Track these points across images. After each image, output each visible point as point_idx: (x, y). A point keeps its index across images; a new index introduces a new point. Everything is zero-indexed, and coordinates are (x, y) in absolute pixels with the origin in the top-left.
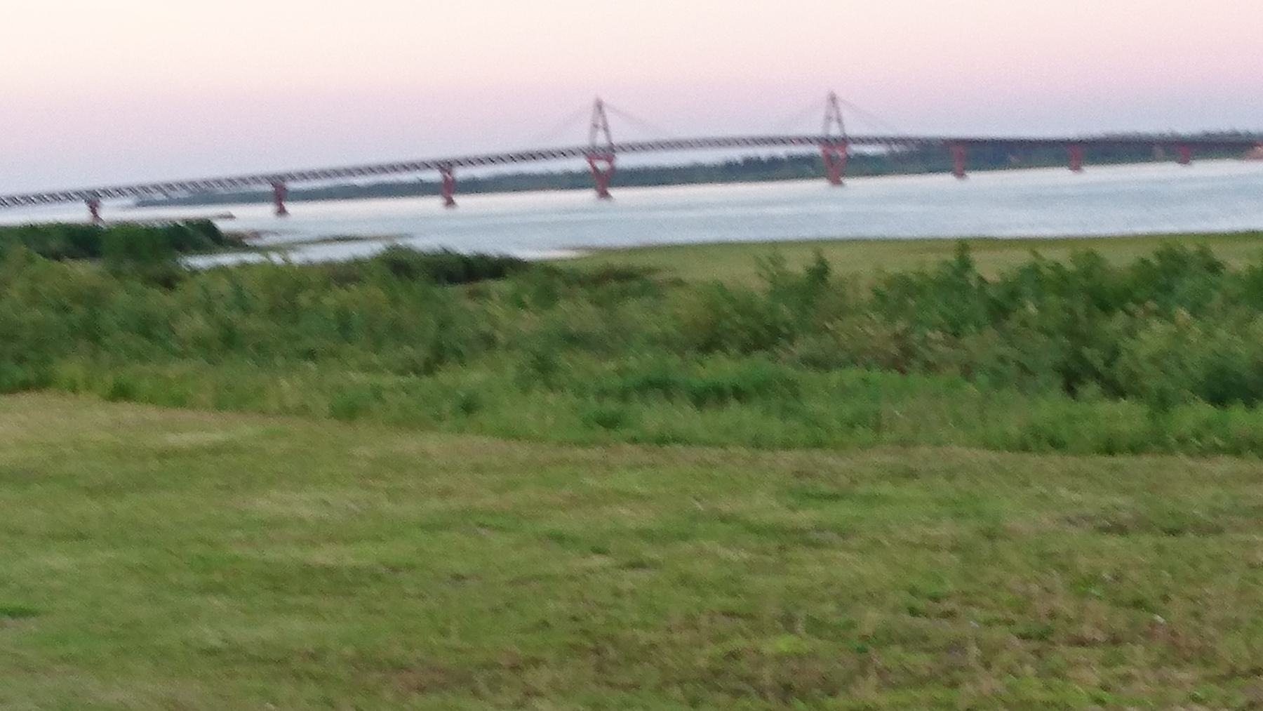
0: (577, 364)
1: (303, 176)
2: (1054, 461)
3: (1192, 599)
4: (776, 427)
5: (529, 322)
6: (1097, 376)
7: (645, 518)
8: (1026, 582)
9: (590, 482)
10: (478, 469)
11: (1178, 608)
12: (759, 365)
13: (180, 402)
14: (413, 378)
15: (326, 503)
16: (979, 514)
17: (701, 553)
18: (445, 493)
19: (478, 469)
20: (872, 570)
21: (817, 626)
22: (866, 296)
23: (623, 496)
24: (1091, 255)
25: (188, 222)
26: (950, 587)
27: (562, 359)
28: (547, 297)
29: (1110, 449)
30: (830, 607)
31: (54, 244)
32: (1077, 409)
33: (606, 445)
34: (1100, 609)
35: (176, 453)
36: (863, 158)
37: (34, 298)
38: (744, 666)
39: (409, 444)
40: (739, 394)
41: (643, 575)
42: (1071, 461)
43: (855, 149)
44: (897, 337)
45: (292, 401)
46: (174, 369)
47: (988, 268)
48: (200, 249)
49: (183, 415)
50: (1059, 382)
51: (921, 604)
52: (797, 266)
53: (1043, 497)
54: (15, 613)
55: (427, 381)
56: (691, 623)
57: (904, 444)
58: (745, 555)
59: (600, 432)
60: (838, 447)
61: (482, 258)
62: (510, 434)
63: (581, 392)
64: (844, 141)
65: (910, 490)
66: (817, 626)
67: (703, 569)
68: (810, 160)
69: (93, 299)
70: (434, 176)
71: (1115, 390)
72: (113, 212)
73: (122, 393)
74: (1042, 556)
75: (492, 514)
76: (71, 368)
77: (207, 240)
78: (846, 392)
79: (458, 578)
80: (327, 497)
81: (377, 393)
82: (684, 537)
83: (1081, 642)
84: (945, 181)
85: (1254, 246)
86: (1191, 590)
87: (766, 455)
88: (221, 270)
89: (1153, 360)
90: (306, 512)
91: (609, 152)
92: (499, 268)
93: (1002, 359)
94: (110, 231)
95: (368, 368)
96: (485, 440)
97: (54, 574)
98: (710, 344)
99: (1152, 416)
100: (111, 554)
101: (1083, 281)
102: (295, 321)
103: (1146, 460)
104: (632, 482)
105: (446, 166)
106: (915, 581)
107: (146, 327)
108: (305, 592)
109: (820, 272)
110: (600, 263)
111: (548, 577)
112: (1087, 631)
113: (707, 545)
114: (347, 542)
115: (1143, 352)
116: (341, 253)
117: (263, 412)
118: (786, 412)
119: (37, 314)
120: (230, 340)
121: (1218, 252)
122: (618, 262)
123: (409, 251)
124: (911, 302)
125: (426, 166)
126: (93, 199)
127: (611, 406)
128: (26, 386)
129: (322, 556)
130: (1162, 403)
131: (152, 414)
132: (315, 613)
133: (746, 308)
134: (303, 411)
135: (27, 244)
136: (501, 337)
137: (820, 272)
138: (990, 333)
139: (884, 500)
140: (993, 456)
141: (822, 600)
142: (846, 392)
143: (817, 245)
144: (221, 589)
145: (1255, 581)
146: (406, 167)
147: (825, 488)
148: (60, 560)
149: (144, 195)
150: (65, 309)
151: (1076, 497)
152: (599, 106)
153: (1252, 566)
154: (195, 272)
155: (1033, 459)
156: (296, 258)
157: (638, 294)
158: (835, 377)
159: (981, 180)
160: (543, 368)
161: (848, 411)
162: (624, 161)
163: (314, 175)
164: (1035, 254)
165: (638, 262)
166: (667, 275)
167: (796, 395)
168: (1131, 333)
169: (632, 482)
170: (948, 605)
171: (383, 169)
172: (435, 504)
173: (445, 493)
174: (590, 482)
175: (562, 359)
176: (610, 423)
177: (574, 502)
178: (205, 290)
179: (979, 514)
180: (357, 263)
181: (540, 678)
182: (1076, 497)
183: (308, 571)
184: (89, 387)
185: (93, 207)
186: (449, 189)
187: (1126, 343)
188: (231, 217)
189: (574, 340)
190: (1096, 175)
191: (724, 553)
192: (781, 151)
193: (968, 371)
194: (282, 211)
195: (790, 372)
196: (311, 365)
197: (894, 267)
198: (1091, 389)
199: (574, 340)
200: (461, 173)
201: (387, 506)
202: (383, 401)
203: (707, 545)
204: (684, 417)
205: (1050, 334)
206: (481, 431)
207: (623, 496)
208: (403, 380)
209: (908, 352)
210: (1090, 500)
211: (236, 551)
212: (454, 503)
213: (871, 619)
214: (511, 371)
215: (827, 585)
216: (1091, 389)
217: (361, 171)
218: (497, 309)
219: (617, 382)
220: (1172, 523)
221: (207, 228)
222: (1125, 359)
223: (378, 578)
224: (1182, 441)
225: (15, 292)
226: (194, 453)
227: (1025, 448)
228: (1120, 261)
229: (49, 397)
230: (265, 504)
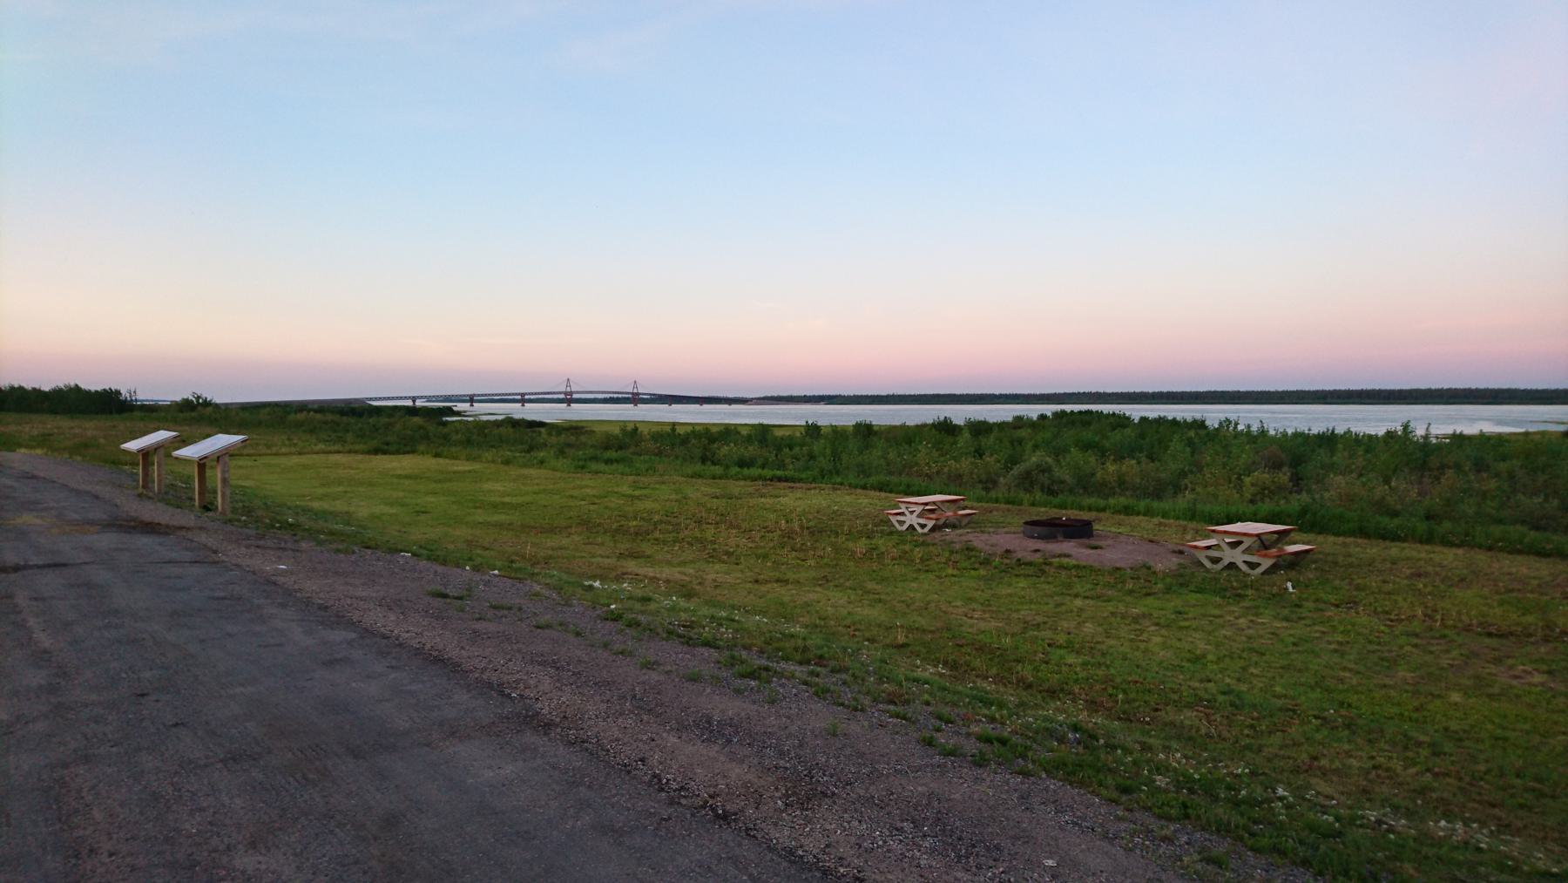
0: (571, 452)
2: (700, 481)
4: (627, 470)
5: (553, 440)
7: (594, 492)
11: (732, 516)
12: (620, 454)
14: (523, 454)
17: (610, 501)
18: (537, 484)
19: (546, 479)
21: (643, 519)
23: (587, 486)
24: (707, 428)
27: (566, 450)
29: (714, 478)
30: (645, 515)
32: (706, 468)
34: (713, 516)
36: (643, 399)
38: (625, 528)
39: (525, 471)
40: (617, 461)
41: (596, 506)
45: (490, 458)
47: (680, 430)
51: (669, 514)
52: (630, 427)
55: (528, 455)
56: (609, 518)
57: (661, 475)
59: (579, 470)
62: (554, 469)
63: (573, 460)
66: (643, 519)
67: (613, 505)
71: (714, 463)
79: (545, 506)
83: (709, 523)
90: (499, 488)
98: (607, 448)
112: (710, 521)
117: (481, 462)
127: (581, 463)
129: (507, 499)
130: (727, 467)
133: (616, 437)
134: (493, 462)
137: (636, 429)
144: (480, 508)
147: (642, 486)
155: (694, 480)
158: (642, 458)
159: (675, 407)
160: (561, 453)
167: (632, 462)
169: (590, 483)
170: (675, 515)
174: (578, 483)
175: (566, 450)
176: (583, 467)
177: (574, 488)
181: (573, 530)
189: (570, 445)
191: (617, 501)
195: (631, 456)
197: (655, 429)
199: (570, 445)
201: (522, 487)
203: (613, 499)
204: (602, 467)
206: (545, 468)
207: (587, 486)
212: (542, 487)
213: (656, 518)
214: (552, 452)
222: (716, 456)
226: (464, 472)
228: (714, 430)
230: (487, 486)
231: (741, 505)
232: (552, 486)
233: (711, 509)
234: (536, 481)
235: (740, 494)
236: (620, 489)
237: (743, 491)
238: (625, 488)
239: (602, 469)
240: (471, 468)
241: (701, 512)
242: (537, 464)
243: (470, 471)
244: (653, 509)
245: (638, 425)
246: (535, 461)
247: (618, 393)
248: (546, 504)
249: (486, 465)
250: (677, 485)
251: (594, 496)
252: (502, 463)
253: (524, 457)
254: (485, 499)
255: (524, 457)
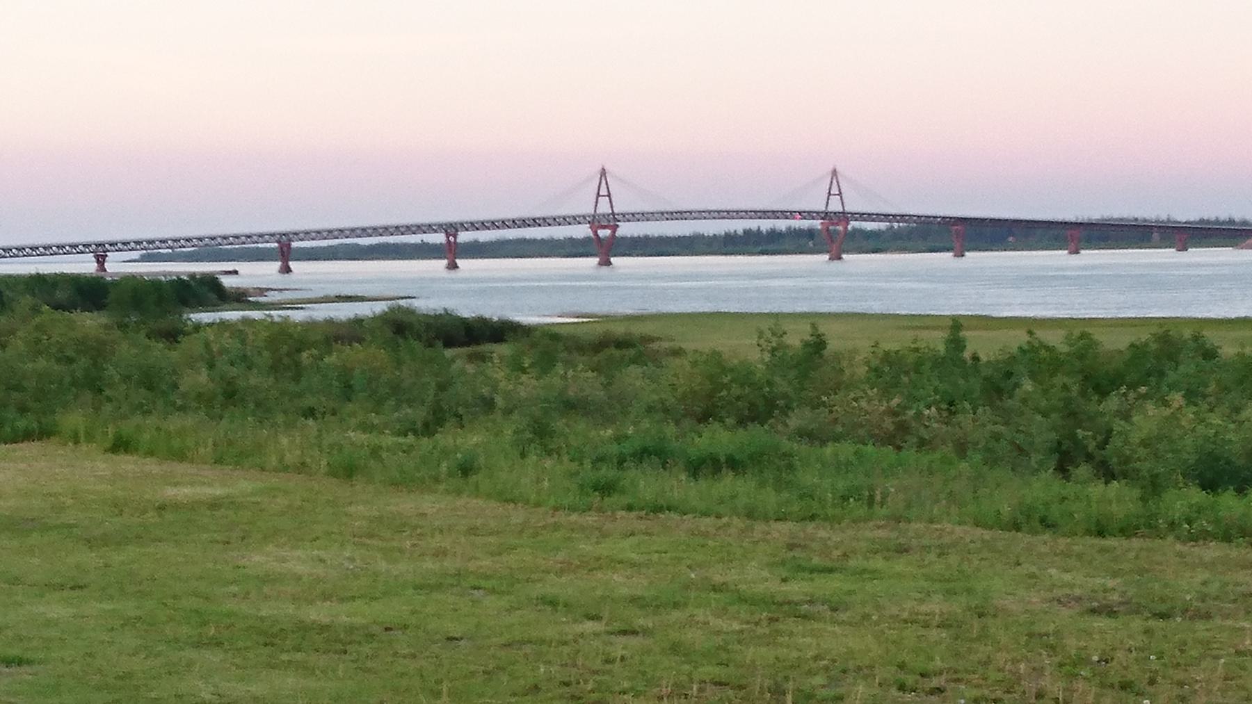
0: (577, 430)
1: (307, 235)
2: (1044, 542)
3: (1181, 684)
4: (770, 498)
5: (529, 386)
6: (1089, 457)
7: (639, 585)
8: (1015, 661)
9: (585, 547)
10: (473, 531)
12: (756, 435)
13: (180, 456)
14: (411, 438)
15: (322, 561)
16: (969, 591)
17: (691, 622)
18: (440, 553)
19: (473, 531)
20: (863, 644)
22: (862, 371)
23: (615, 563)
24: (1083, 336)
25: (192, 276)
26: (938, 663)
27: (559, 424)
28: (546, 362)
30: (819, 680)
31: (60, 295)
32: (1070, 489)
33: (600, 510)
35: (176, 506)
37: (37, 349)
39: (405, 504)
40: (734, 464)
41: (634, 641)
42: (1063, 542)
43: (853, 224)
44: (893, 413)
46: (175, 422)
47: (982, 346)
48: (204, 305)
49: (180, 468)
50: (1052, 463)
51: (910, 680)
52: (796, 339)
53: (1032, 576)
54: (8, 662)
55: (425, 441)
58: (736, 626)
59: (596, 498)
60: (833, 520)
61: (483, 322)
62: (506, 497)
63: (578, 458)
64: (844, 217)
65: (901, 565)
67: (694, 637)
68: (811, 234)
69: (97, 351)
70: (439, 238)
71: (1107, 473)
72: (117, 265)
73: (121, 445)
74: (1031, 635)
75: (487, 577)
76: (74, 419)
77: (213, 296)
78: (842, 467)
80: (322, 554)
81: (375, 452)
82: (676, 605)
84: (944, 259)
85: (1246, 333)
86: (1180, 675)
87: (759, 527)
88: (223, 324)
89: (1145, 443)
90: (300, 569)
91: (613, 220)
92: (501, 331)
93: (997, 437)
94: (115, 284)
95: (366, 427)
96: (481, 502)
97: (49, 623)
99: (1143, 499)
100: (107, 606)
101: (1078, 364)
102: (297, 378)
103: (1136, 543)
104: (625, 548)
105: (451, 229)
106: (906, 657)
107: (149, 380)
108: (298, 649)
109: (818, 345)
110: (600, 329)
111: (543, 642)
113: (700, 615)
114: (342, 600)
115: (1135, 438)
116: (344, 312)
118: (779, 485)
119: (42, 363)
120: (231, 395)
121: (1212, 337)
122: (619, 330)
123: (410, 312)
124: (905, 379)
125: (430, 228)
126: (100, 252)
127: (607, 472)
128: (28, 436)
129: (317, 613)
130: (1154, 487)
131: (152, 466)
132: (307, 670)
133: (745, 376)
134: (302, 468)
135: (34, 295)
136: (499, 401)
137: (818, 345)
138: (984, 413)
139: (874, 574)
140: (987, 535)
141: (810, 673)
142: (842, 467)
143: (813, 318)
145: (1244, 668)
146: (409, 229)
147: (816, 561)
148: (57, 609)
149: (150, 249)
150: (70, 360)
151: (1067, 577)
152: (603, 173)
153: (1239, 653)
154: (198, 327)
156: (297, 316)
157: (634, 361)
158: (829, 450)
161: (841, 485)
162: (627, 230)
163: (319, 234)
164: (1030, 333)
165: (638, 330)
166: (666, 345)
167: (790, 467)
168: (1126, 416)
169: (625, 548)
170: (935, 682)
171: (386, 230)
172: (429, 564)
173: (440, 553)
174: (585, 547)
175: (559, 424)
176: (606, 489)
178: (207, 345)
179: (969, 591)
180: (358, 322)
182: (1067, 577)
183: (303, 628)
184: (90, 437)
185: (101, 260)
186: (452, 252)
187: (1118, 425)
188: (236, 272)
189: (571, 406)
190: (1090, 257)
191: (716, 623)
192: (782, 225)
193: (962, 449)
194: (286, 270)
195: (786, 445)
196: (311, 422)
198: (1083, 471)
199: (571, 406)
200: (464, 237)
201: (383, 565)
202: (381, 460)
203: (700, 615)
204: (678, 486)
205: (1045, 415)
206: (477, 492)
207: (615, 563)
208: (401, 440)
209: (903, 428)
210: (1079, 581)
211: (230, 605)
212: (449, 564)
214: (508, 432)
215: (816, 658)
216: (1083, 471)
217: (364, 232)
218: (499, 374)
219: (614, 449)
220: (1162, 608)
221: (211, 282)
222: (1116, 442)
223: (371, 637)
224: (1172, 525)
225: (18, 344)
226: (193, 506)
227: (1017, 527)
229: (50, 446)
230: (260, 560)
231: (1206, 643)
232: (486, 562)
233: (1082, 661)
234: (437, 541)
235: (1203, 598)
236: (732, 576)
237: (1213, 589)
238: (753, 569)
239: (676, 495)
240: (219, 491)
241: (1038, 671)
242: (450, 474)
243: (214, 505)
244: (851, 653)
245: (822, 330)
246: (444, 466)
247: (775, 214)
248: (455, 629)
249: (274, 480)
250: (953, 559)
251: (634, 600)
252: (333, 473)
253: (408, 451)
254: (244, 608)
255: (408, 451)
